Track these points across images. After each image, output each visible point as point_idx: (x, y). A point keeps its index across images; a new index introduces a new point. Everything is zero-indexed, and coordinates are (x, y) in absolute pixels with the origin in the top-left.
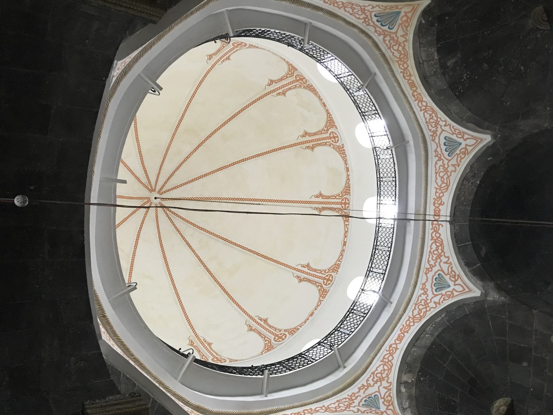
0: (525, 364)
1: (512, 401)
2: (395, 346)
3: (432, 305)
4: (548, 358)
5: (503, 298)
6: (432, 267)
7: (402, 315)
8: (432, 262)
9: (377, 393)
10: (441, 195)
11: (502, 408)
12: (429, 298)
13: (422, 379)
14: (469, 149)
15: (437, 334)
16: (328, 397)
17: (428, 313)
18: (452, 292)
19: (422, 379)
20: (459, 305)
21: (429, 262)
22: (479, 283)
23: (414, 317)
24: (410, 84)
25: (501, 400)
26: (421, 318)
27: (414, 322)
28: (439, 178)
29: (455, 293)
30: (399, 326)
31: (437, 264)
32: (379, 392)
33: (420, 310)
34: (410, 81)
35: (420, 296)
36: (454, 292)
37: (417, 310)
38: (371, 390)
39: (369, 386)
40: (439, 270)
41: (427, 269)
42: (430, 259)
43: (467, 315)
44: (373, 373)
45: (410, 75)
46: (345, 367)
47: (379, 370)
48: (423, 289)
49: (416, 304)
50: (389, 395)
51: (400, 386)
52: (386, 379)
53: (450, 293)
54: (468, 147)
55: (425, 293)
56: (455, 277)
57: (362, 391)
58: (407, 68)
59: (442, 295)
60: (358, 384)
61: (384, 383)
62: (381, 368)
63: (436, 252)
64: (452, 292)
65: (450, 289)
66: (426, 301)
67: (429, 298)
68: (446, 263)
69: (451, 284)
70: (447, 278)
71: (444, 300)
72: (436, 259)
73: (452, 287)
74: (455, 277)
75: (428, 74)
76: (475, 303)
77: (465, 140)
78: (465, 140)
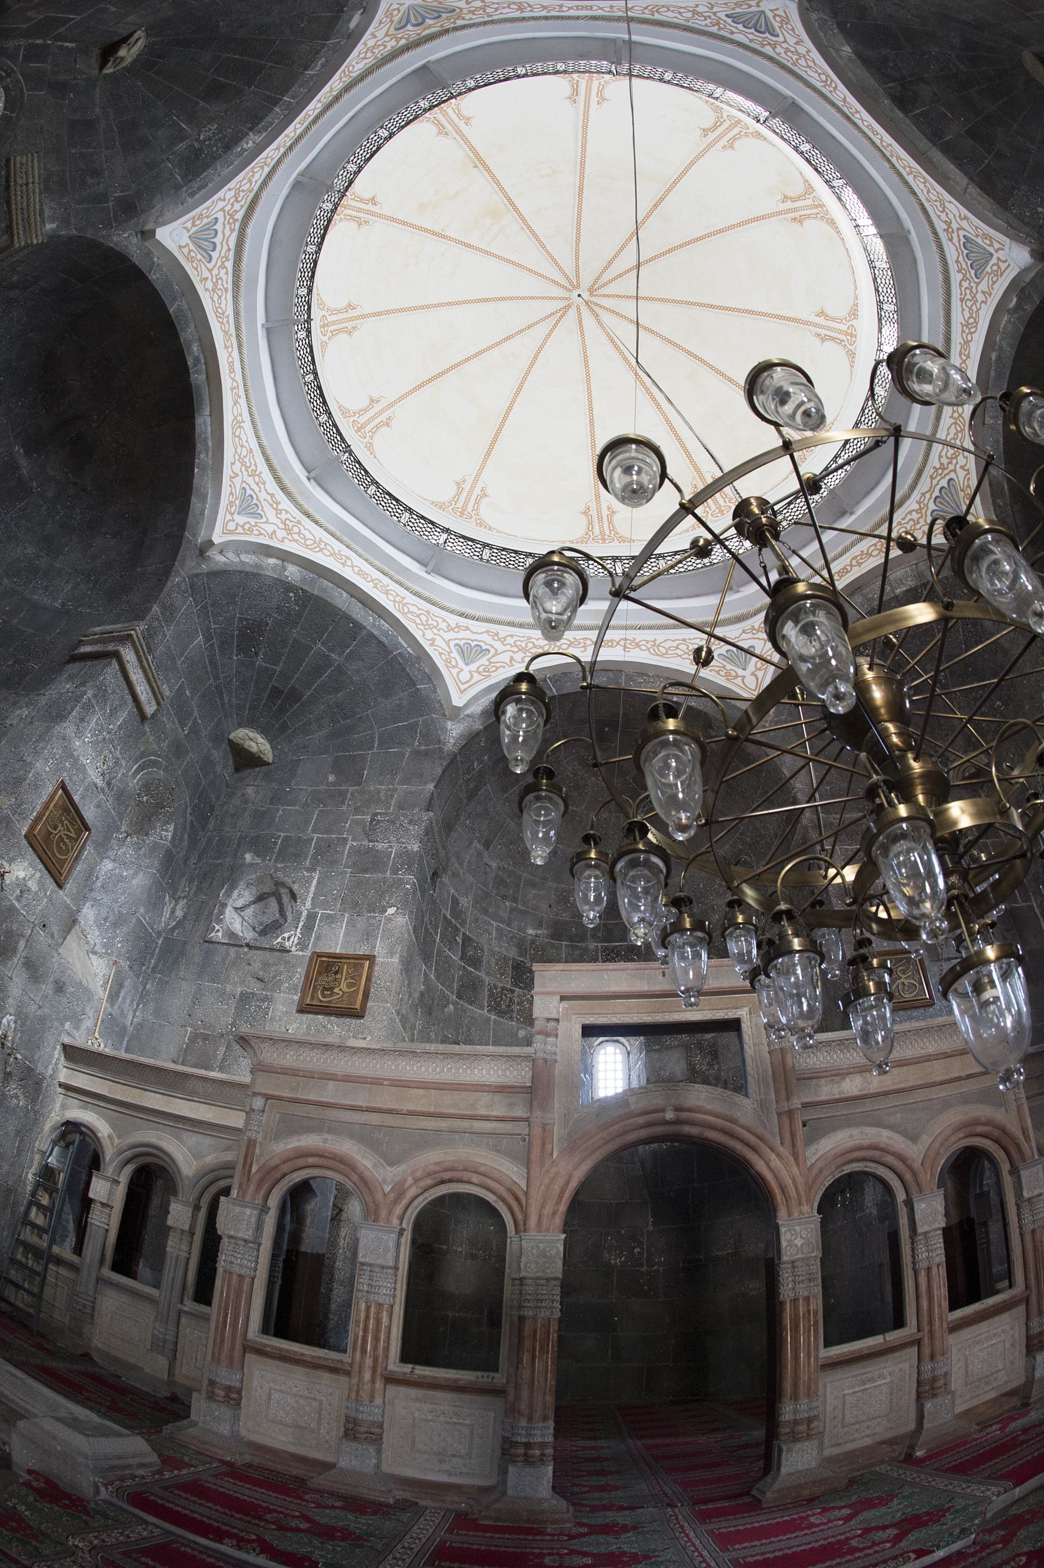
0: (331, 778)
1: (267, 764)
2: (349, 563)
3: (429, 634)
4: (344, 808)
5: (452, 741)
6: (503, 640)
7: (407, 589)
8: (509, 640)
9: (264, 519)
10: (644, 648)
11: (254, 745)
12: (441, 633)
13: (291, 595)
14: (739, 681)
15: (376, 633)
16: (258, 437)
17: (414, 625)
18: (456, 666)
19: (291, 595)
20: (433, 675)
21: (512, 636)
22: (477, 708)
23: (405, 605)
24: (845, 568)
25: (268, 746)
26: (403, 613)
27: (395, 601)
28: (675, 644)
29: (455, 671)
30: (386, 580)
31: (508, 647)
32: (267, 522)
33: (418, 616)
34: (849, 568)
35: (444, 621)
36: (457, 670)
37: (418, 612)
38: (270, 513)
39: (278, 512)
40: (496, 650)
41: (497, 634)
42: (515, 638)
43: (414, 685)
44: (299, 522)
45: (859, 564)
46: (309, 479)
47: (303, 531)
48: (457, 626)
49: (428, 612)
50: (260, 534)
51: (278, 558)
52: (290, 537)
53: (454, 663)
54: (740, 679)
55: (450, 629)
56: (484, 671)
57: (268, 498)
58: (871, 555)
59: (449, 653)
60: (280, 496)
61: (280, 534)
62: (308, 535)
63: (530, 645)
64: (456, 666)
65: (461, 664)
66: (435, 627)
67: (441, 633)
68: (512, 658)
69: (473, 667)
70: (484, 661)
71: (440, 654)
72: (516, 646)
73: (467, 669)
74: (486, 672)
75: (865, 591)
76: (439, 702)
77: (753, 674)
78: (753, 674)
